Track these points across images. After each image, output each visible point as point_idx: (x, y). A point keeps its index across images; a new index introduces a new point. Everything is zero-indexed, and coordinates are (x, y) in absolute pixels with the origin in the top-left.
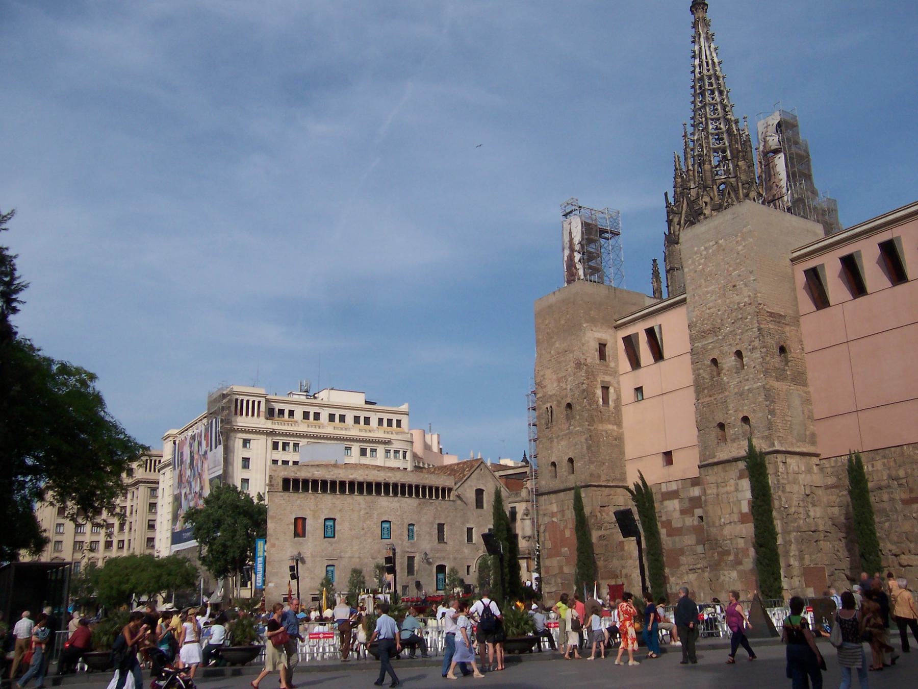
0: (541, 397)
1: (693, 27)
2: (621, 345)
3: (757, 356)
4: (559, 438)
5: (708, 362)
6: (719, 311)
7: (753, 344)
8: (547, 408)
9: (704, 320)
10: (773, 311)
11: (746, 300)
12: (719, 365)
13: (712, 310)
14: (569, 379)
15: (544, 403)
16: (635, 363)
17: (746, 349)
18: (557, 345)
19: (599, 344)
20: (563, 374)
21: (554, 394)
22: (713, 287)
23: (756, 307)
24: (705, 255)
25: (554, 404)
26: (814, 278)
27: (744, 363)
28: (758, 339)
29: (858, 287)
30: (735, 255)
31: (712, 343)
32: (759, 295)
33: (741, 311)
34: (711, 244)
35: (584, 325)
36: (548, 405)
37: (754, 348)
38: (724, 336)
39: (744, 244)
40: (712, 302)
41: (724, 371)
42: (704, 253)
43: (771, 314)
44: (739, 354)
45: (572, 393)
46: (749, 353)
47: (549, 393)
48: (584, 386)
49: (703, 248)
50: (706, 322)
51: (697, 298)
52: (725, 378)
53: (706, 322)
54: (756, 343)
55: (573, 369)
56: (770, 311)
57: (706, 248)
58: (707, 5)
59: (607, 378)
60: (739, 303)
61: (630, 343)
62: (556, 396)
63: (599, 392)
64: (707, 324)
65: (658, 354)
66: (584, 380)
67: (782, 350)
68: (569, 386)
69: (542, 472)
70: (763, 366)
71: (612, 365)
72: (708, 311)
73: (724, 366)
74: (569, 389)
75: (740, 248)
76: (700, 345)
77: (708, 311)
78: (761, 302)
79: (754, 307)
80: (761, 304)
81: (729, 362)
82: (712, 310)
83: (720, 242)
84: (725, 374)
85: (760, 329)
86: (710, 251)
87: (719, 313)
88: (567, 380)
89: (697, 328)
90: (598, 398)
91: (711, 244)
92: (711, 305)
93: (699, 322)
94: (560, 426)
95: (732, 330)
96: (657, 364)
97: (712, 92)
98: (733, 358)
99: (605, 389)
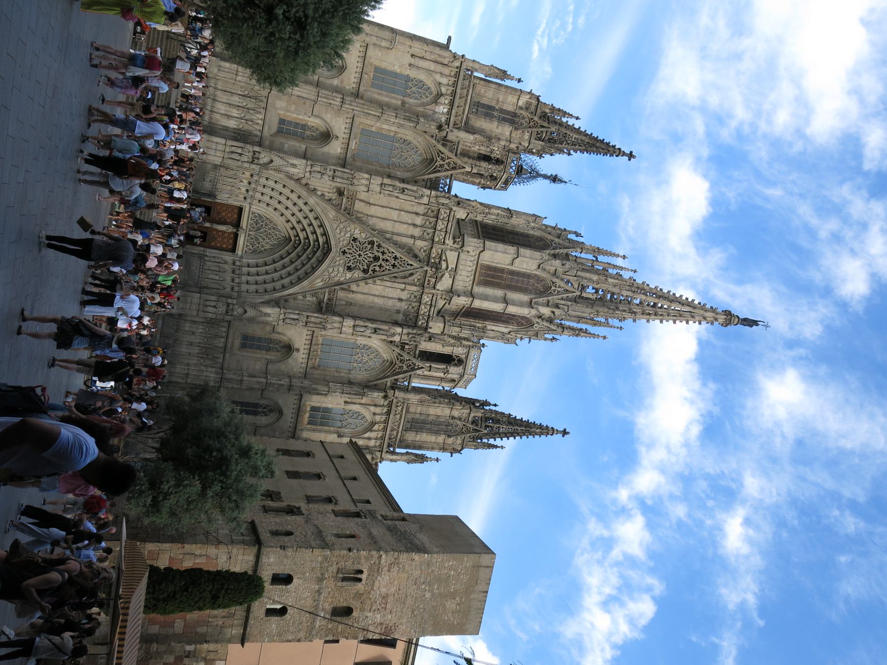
0: (379, 563)
4: (317, 594)
8: (361, 572)
14: (378, 616)
15: (370, 569)
20: (389, 606)
21: (372, 589)
25: (360, 586)
36: (364, 576)
45: (361, 619)
47: (379, 578)
55: (388, 622)
62: (369, 593)
69: (286, 557)
74: (368, 614)
88: (380, 613)
94: (331, 593)
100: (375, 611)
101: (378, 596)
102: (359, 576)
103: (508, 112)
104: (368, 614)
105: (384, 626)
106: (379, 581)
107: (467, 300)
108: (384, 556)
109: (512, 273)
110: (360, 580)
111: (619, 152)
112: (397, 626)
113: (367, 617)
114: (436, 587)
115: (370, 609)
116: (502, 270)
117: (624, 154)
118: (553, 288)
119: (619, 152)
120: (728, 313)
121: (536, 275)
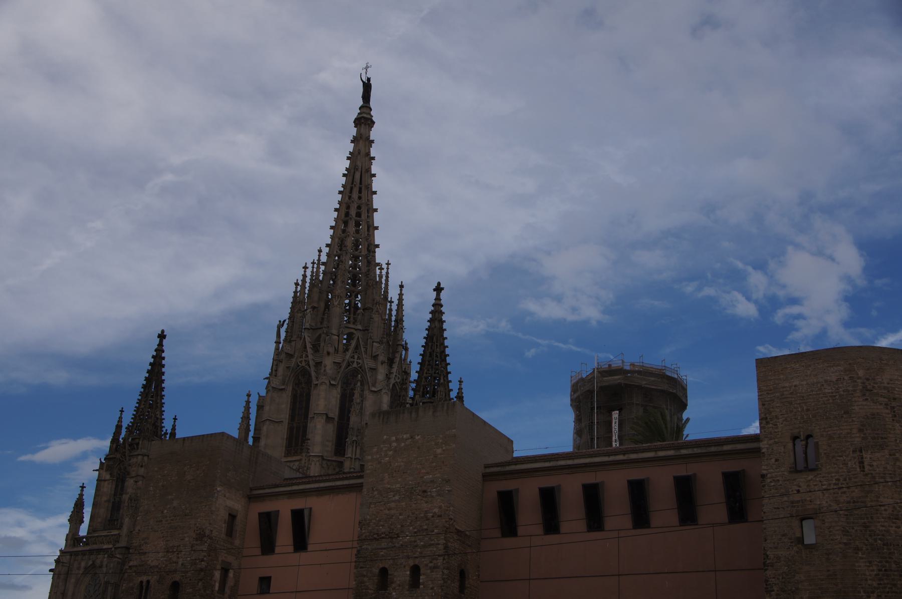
0: (136, 566)
1: (352, 142)
2: (254, 518)
3: (438, 576)
5: (376, 571)
6: (400, 515)
7: (435, 561)
9: (380, 521)
10: (460, 529)
11: (436, 510)
12: (389, 577)
13: (393, 512)
16: (268, 546)
17: (427, 565)
18: (175, 503)
19: (230, 514)
21: (157, 566)
22: (398, 486)
23: (446, 522)
24: (396, 447)
26: (507, 501)
27: (421, 581)
28: (442, 558)
29: (551, 524)
30: (432, 457)
31: (384, 549)
32: (451, 508)
33: (427, 522)
34: (405, 436)
35: (218, 489)
36: (144, 578)
37: (436, 567)
38: (402, 545)
39: (444, 448)
40: (393, 501)
41: (393, 585)
42: (394, 444)
43: (458, 532)
44: (416, 571)
46: (429, 571)
48: (204, 564)
49: (394, 438)
50: (381, 523)
51: (376, 493)
52: (394, 594)
53: (381, 523)
54: (440, 561)
56: (458, 528)
57: (397, 440)
58: (373, 123)
59: (230, 559)
60: (426, 512)
61: (268, 522)
63: (217, 575)
64: (383, 526)
65: (300, 542)
66: (205, 556)
67: (462, 574)
68: (181, 559)
70: (442, 590)
71: (237, 542)
72: (387, 512)
73: (395, 579)
74: (180, 563)
75: (439, 451)
76: (369, 547)
77: (387, 512)
78: (452, 517)
79: (444, 520)
80: (451, 519)
81: (402, 576)
82: (393, 512)
83: (417, 438)
84: (394, 589)
85: (446, 547)
86: (403, 444)
87: (400, 517)
89: (370, 528)
90: (215, 582)
91: (405, 436)
92: (393, 505)
93: (374, 521)
95: (413, 539)
96: (297, 555)
97: (358, 224)
98: (408, 573)
99: (225, 571)
100: (178, 558)
101: (165, 559)
102: (144, 584)
103: (117, 486)
104: (180, 563)
105: (195, 542)
106: (152, 561)
107: (313, 463)
108: (131, 564)
109: (292, 418)
110: (148, 582)
111: (160, 350)
112: (197, 527)
113: (182, 564)
114: (170, 497)
115: (175, 563)
116: (291, 429)
117: (161, 344)
118: (304, 364)
119: (160, 350)
120: (358, 122)
121: (293, 389)
